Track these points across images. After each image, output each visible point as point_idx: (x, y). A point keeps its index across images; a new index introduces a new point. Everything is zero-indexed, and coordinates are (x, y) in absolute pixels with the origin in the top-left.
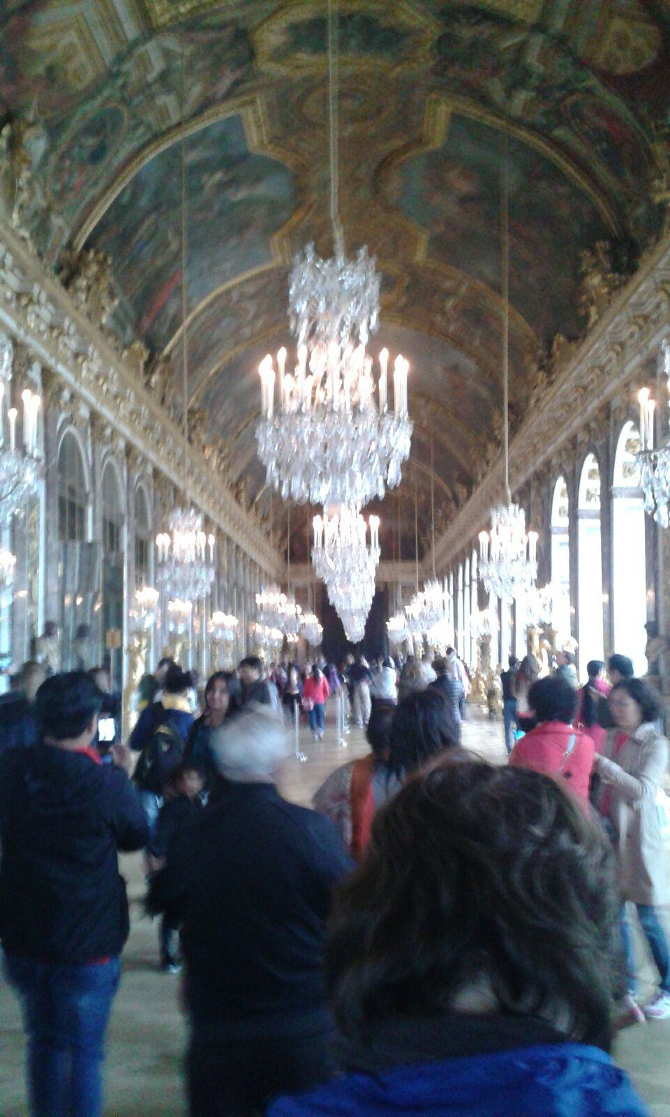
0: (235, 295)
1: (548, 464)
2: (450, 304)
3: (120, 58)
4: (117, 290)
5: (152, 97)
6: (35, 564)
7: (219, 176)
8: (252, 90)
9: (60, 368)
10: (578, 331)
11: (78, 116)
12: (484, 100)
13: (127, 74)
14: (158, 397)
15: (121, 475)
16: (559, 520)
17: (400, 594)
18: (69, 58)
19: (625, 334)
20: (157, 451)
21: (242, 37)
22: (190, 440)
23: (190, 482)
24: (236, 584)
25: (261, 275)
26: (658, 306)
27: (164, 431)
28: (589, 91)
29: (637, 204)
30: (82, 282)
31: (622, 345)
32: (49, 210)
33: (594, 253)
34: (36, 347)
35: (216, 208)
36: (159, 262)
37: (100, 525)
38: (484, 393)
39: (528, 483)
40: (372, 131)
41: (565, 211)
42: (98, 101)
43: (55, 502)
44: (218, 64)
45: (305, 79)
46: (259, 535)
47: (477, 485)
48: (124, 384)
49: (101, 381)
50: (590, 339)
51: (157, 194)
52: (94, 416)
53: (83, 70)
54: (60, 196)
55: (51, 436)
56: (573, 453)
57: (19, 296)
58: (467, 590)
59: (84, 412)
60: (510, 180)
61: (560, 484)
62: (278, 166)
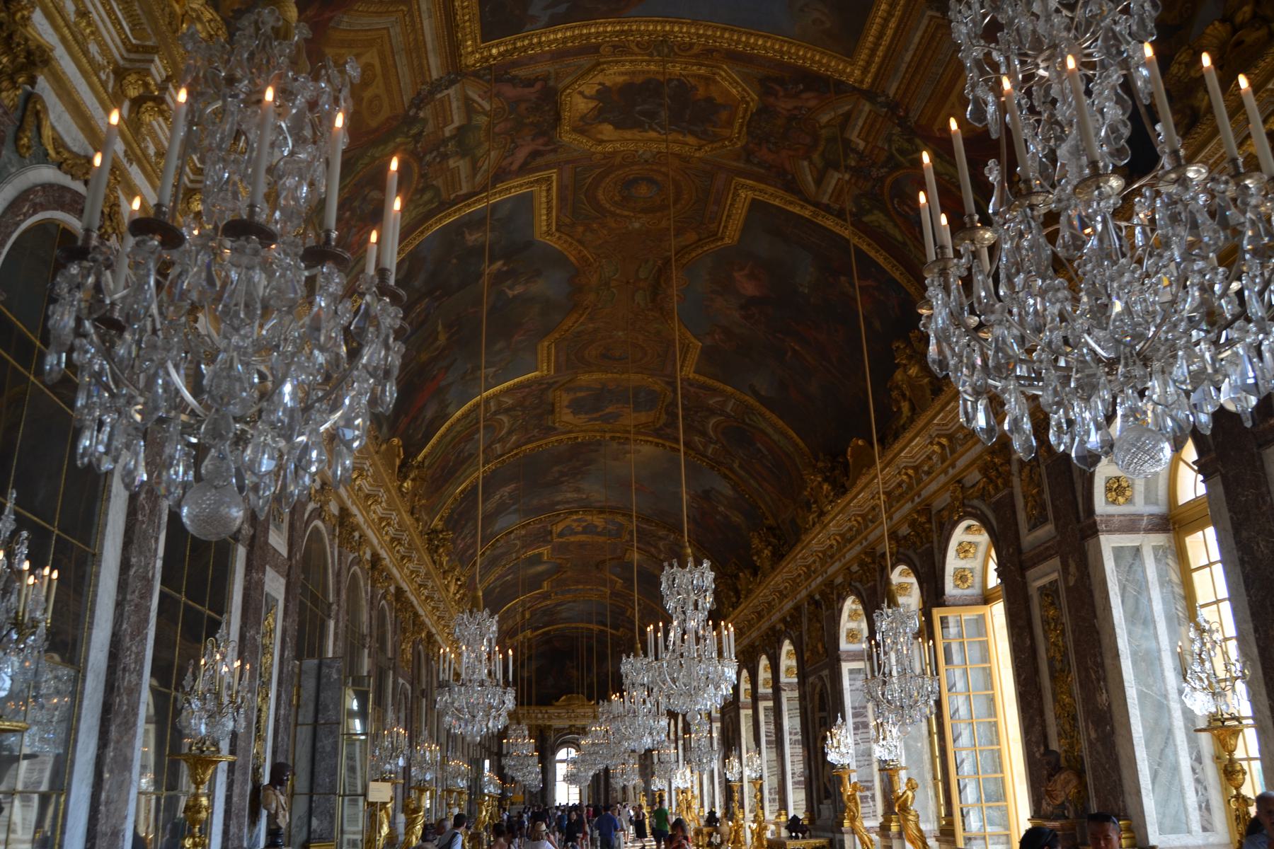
2: (713, 421)
3: (419, 101)
5: (445, 157)
6: (266, 684)
11: (366, 160)
13: (425, 121)
20: (400, 568)
21: (550, 98)
22: (434, 562)
25: (521, 386)
27: (411, 546)
37: (340, 644)
38: (737, 518)
39: (797, 608)
45: (607, 156)
59: (334, 508)
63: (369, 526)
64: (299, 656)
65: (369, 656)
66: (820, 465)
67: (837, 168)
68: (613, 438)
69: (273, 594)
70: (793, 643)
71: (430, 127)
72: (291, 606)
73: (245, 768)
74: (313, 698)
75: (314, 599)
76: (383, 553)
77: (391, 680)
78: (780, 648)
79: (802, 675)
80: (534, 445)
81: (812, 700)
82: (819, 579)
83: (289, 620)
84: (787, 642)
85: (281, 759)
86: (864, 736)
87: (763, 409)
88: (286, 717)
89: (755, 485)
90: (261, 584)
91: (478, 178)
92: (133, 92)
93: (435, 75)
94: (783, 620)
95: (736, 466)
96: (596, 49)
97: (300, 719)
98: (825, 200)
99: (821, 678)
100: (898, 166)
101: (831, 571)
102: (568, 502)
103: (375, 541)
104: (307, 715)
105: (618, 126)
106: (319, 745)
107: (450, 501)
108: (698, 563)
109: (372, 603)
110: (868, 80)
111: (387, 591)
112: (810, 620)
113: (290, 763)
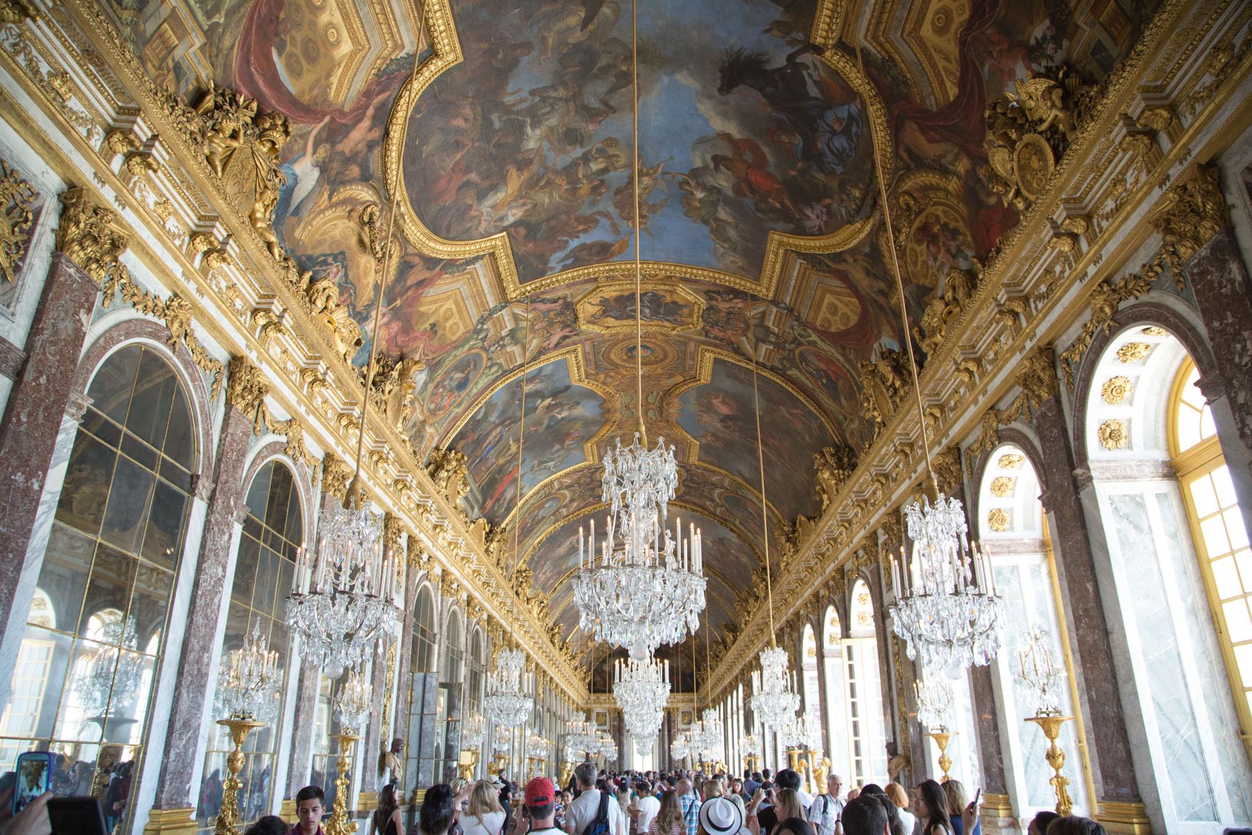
0: (556, 485)
1: (797, 614)
2: (717, 492)
3: (483, 321)
4: (470, 480)
5: (504, 346)
7: (548, 401)
8: (574, 343)
9: (422, 537)
10: (816, 514)
12: (738, 351)
14: (495, 560)
15: (462, 619)
16: (809, 660)
17: (680, 719)
18: (447, 320)
19: (851, 514)
20: (491, 603)
21: (569, 307)
22: (517, 594)
23: (516, 626)
24: (549, 710)
25: (576, 471)
26: (874, 493)
28: (814, 343)
29: (852, 420)
30: (443, 474)
31: (850, 522)
32: (424, 422)
33: (823, 455)
34: (406, 520)
35: (546, 422)
36: (501, 461)
37: (443, 660)
38: (744, 559)
40: (659, 371)
41: (799, 427)
42: (467, 347)
43: (409, 640)
44: (551, 323)
46: (568, 670)
47: (742, 630)
48: (470, 550)
50: (825, 518)
51: (503, 412)
53: (456, 328)
54: (433, 413)
56: (818, 604)
57: (396, 482)
58: (735, 717)
59: (438, 571)
60: (758, 405)
61: (808, 631)
62: (591, 395)
67: (764, 342)
71: (492, 332)
73: (375, 741)
75: (423, 632)
76: (476, 594)
85: (399, 736)
88: (403, 710)
91: (528, 354)
92: (309, 380)
93: (492, 305)
95: (737, 522)
96: (596, 279)
98: (761, 360)
100: (800, 344)
104: (416, 708)
105: (616, 318)
110: (771, 295)
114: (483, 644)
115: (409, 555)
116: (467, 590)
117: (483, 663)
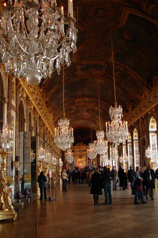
15: (32, 115)
20: (40, 111)
24: (54, 150)
37: (28, 129)
39: (138, 120)
43: (18, 120)
49: (29, 87)
52: (27, 96)
55: (18, 99)
59: (25, 95)
63: (33, 100)
64: (19, 132)
65: (34, 132)
66: (145, 84)
68: (92, 78)
69: (13, 116)
70: (137, 129)
72: (17, 119)
73: (10, 157)
74: (23, 141)
75: (22, 118)
77: (39, 138)
78: (133, 130)
79: (139, 137)
80: (71, 80)
81: (142, 143)
82: (144, 113)
83: (17, 122)
84: (135, 129)
85: (17, 155)
86: (155, 151)
87: (131, 70)
88: (18, 145)
89: (127, 89)
90: (10, 113)
94: (134, 123)
95: (123, 84)
97: (20, 147)
98: (149, 13)
99: (144, 137)
101: (147, 111)
102: (79, 95)
103: (34, 104)
104: (22, 145)
106: (25, 152)
107: (51, 94)
108: (118, 107)
109: (34, 119)
111: (37, 117)
112: (141, 123)
113: (19, 156)
114: (38, 125)
115: (16, 86)
116: (34, 105)
117: (38, 132)
